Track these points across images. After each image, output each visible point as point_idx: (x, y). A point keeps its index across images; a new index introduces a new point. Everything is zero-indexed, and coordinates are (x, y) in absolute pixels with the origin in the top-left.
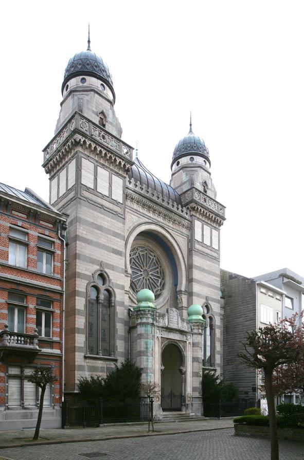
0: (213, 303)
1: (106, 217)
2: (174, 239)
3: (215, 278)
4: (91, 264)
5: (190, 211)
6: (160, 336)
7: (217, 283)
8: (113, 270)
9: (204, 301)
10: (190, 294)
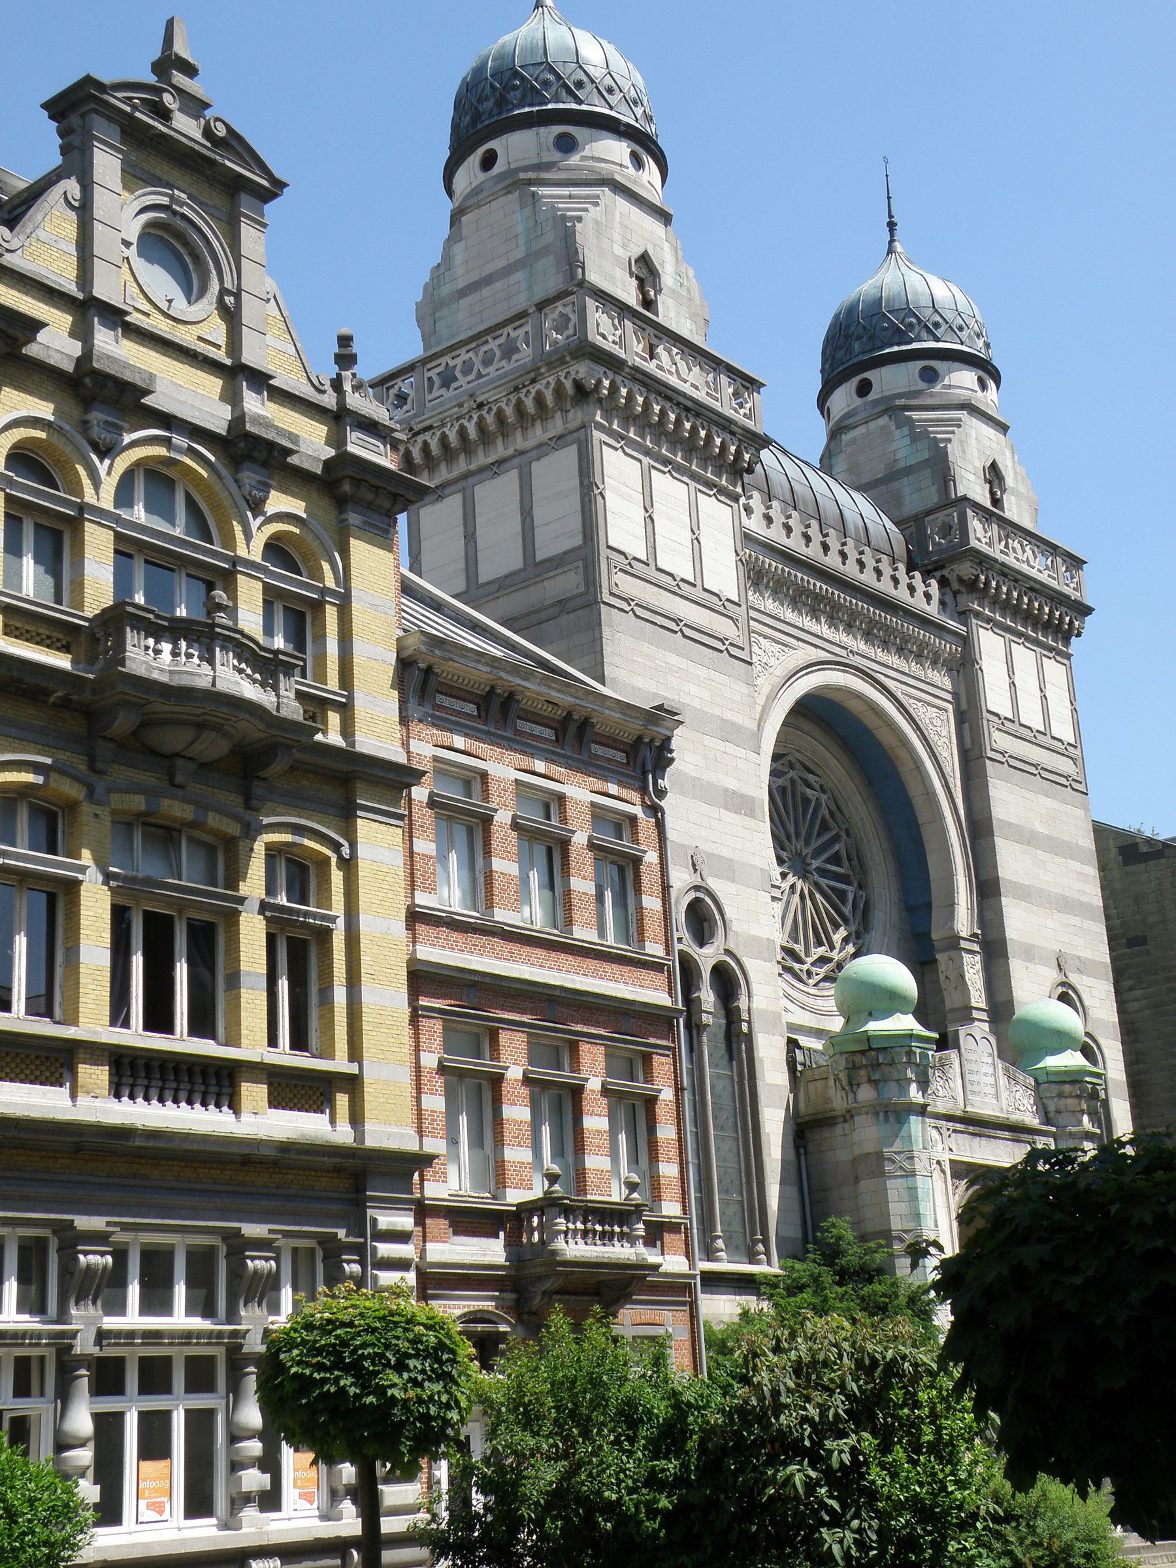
2: (918, 728)
5: (955, 593)
6: (946, 1157)
8: (733, 881)
9: (1053, 976)
10: (994, 949)
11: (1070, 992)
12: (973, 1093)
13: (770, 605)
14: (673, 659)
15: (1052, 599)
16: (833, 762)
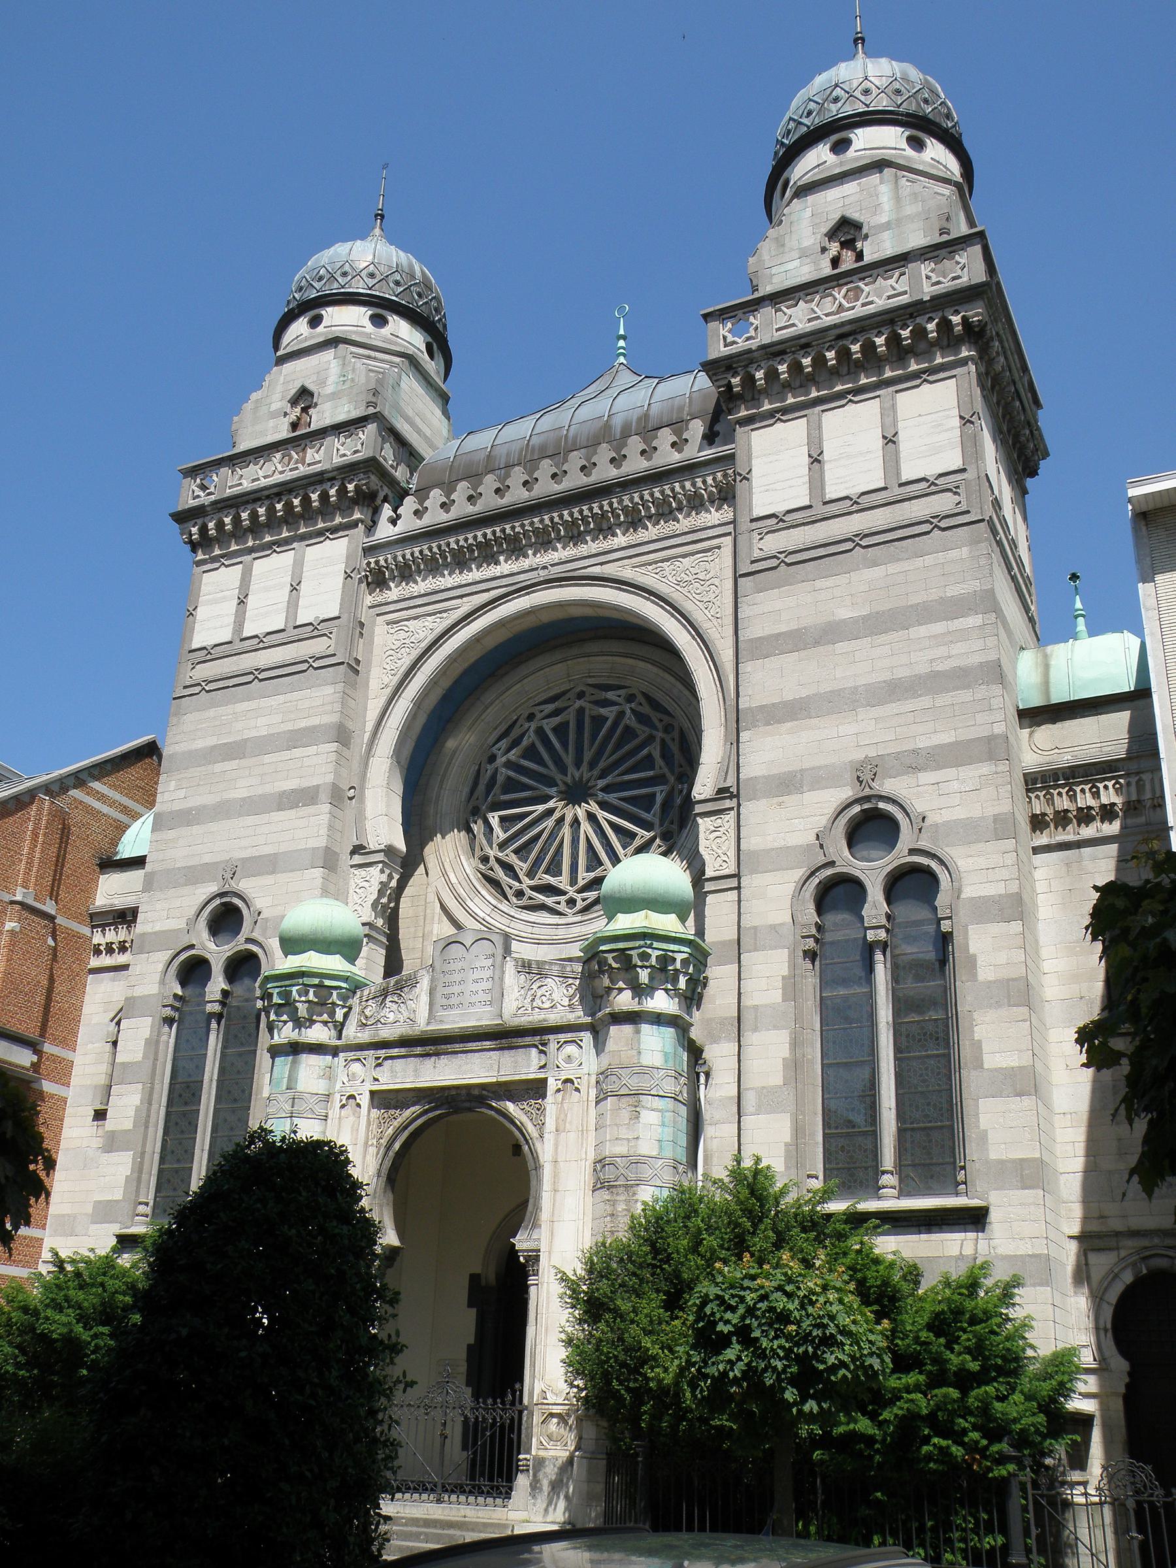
1: (264, 702)
3: (938, 628)
4: (186, 890)
7: (958, 648)
8: (273, 873)
11: (881, 805)
12: (450, 1007)
13: (422, 585)
14: (241, 707)
15: (892, 322)
16: (641, 664)
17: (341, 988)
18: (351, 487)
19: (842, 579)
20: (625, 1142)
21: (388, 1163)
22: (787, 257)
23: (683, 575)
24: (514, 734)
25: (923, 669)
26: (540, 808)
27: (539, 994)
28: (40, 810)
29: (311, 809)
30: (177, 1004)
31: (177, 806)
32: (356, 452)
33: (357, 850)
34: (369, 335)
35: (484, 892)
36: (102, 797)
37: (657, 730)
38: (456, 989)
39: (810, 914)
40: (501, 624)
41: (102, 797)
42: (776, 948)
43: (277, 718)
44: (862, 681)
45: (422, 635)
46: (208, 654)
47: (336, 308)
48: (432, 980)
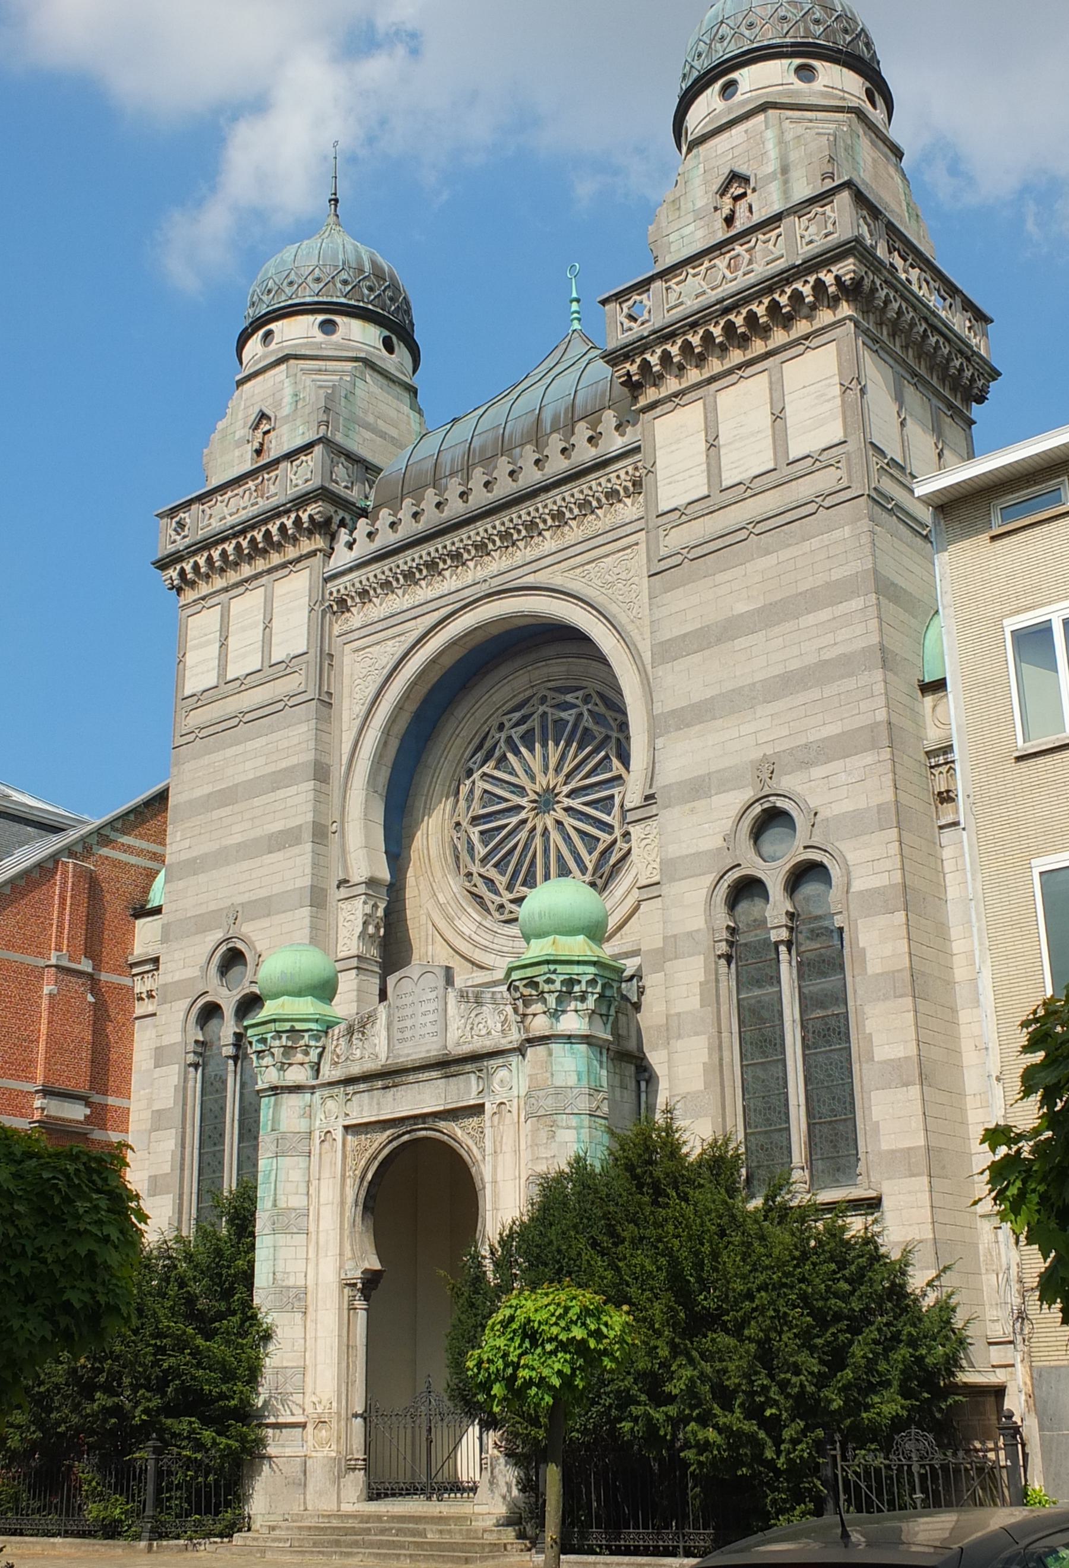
0: (817, 772)
1: (250, 745)
3: (824, 615)
7: (843, 634)
12: (405, 1040)
17: (312, 1030)
18: (305, 517)
19: (738, 571)
20: (544, 1161)
21: (363, 1193)
22: (683, 221)
23: (607, 577)
24: (488, 745)
25: (812, 659)
26: (514, 820)
27: (476, 1023)
28: (65, 873)
29: (296, 850)
30: (199, 1050)
31: (184, 856)
32: (307, 481)
33: (343, 883)
34: (319, 345)
35: (470, 910)
36: (128, 849)
37: (612, 729)
38: (409, 1023)
39: (722, 919)
40: (454, 643)
41: (128, 849)
42: (693, 955)
43: (261, 761)
44: (759, 676)
45: (384, 662)
46: (200, 699)
47: (285, 321)
48: (389, 1016)
